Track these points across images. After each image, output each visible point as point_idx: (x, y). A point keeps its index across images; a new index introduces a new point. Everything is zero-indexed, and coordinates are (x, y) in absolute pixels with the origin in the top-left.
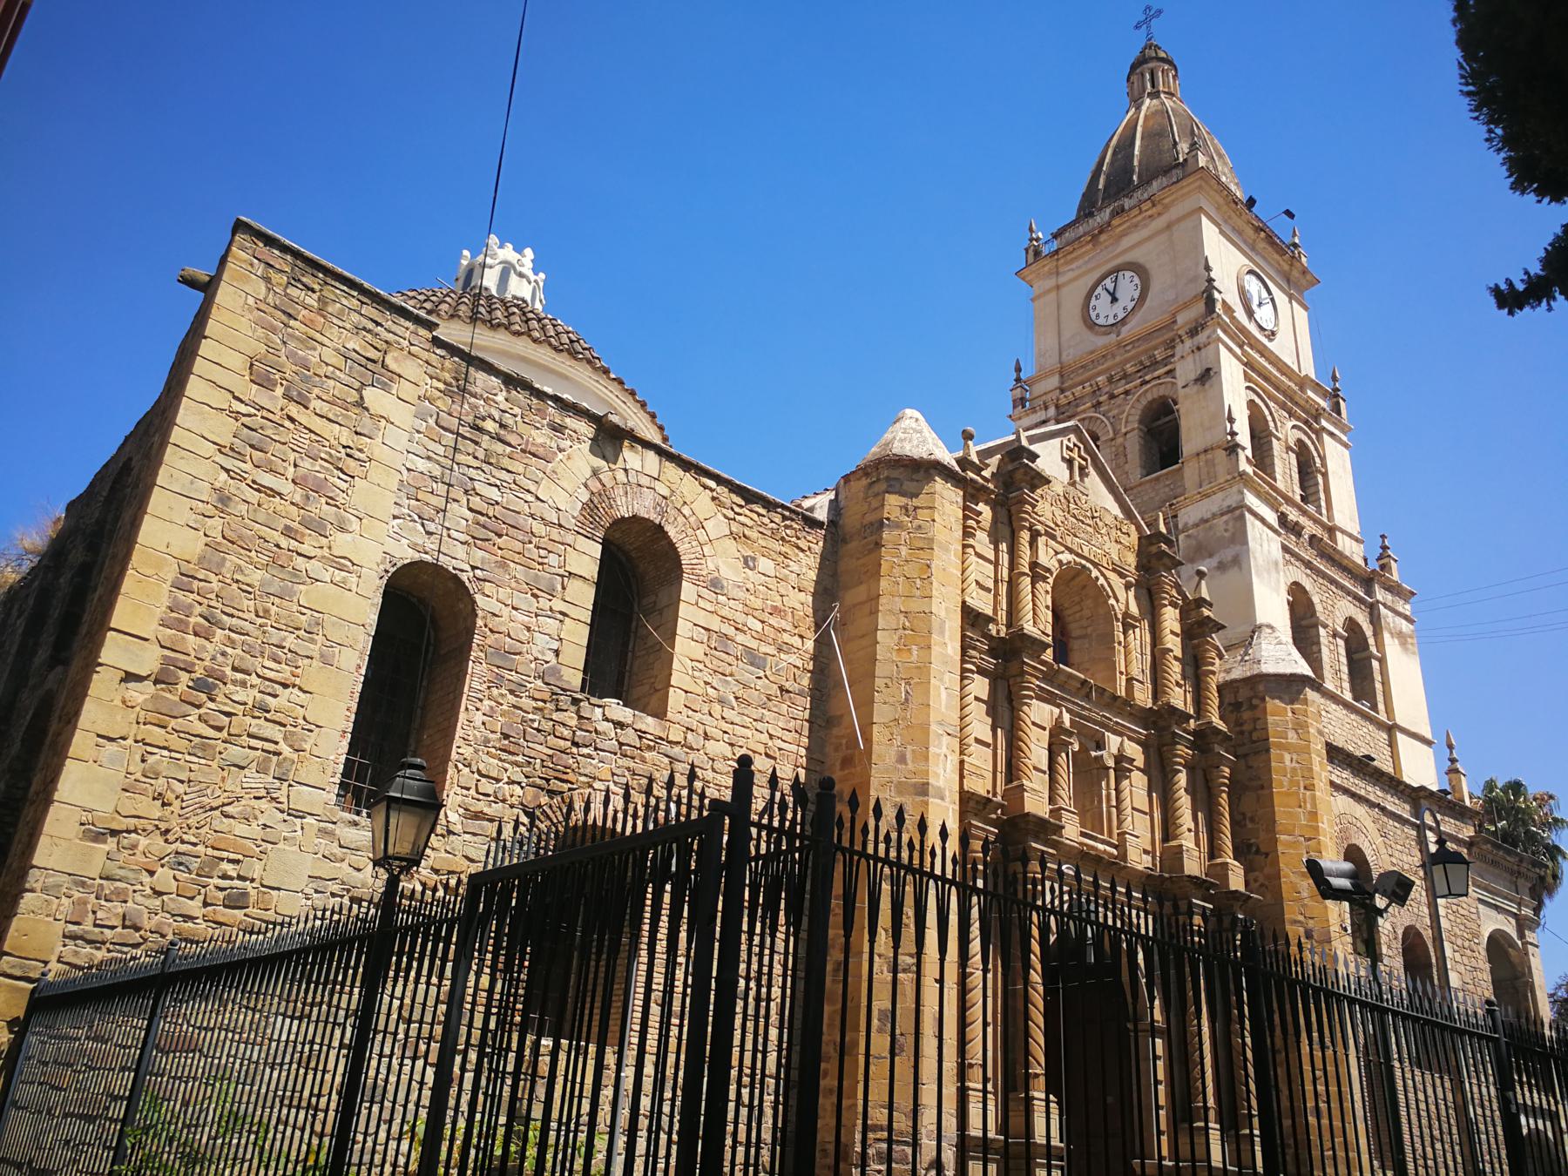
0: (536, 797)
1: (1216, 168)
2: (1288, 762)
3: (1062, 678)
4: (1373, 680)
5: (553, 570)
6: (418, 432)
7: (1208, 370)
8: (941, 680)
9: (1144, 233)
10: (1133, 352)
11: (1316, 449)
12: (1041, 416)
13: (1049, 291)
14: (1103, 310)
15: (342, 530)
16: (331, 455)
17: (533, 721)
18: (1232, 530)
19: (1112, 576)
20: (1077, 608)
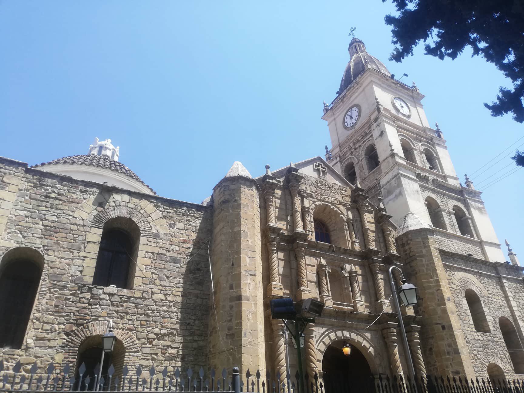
0: (71, 327)
1: (379, 69)
2: (424, 262)
3: (320, 246)
4: (470, 226)
5: (81, 242)
6: (21, 202)
7: (382, 132)
8: (246, 254)
9: (357, 94)
11: (433, 150)
12: (335, 161)
13: (332, 121)
14: (349, 122)
17: (70, 299)
18: (397, 183)
19: (341, 207)
20: (330, 220)
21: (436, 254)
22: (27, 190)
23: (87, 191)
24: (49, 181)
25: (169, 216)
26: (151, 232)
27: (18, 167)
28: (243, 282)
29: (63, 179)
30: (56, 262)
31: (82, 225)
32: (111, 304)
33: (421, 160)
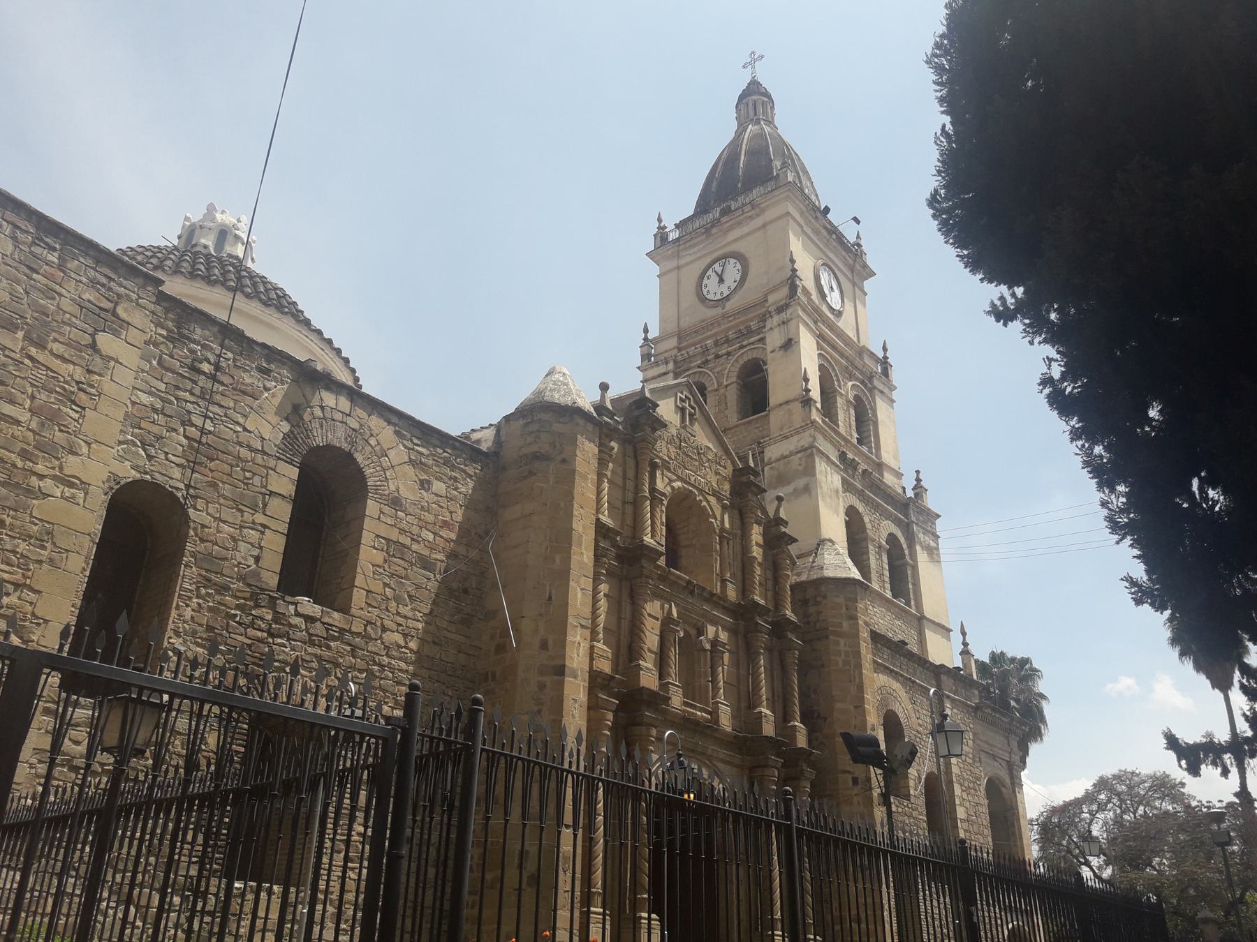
1: (801, 182)
7: (790, 340)
8: (578, 582)
9: (746, 229)
10: (734, 322)
12: (662, 369)
14: (713, 289)
15: (73, 453)
16: (64, 389)
17: (236, 615)
19: (712, 500)
21: (864, 634)
22: (156, 345)
23: (272, 371)
24: (198, 333)
25: (421, 462)
26: (387, 493)
27: (144, 287)
28: (569, 638)
29: (229, 333)
30: (210, 528)
31: (259, 450)
32: (310, 639)
33: (846, 419)
